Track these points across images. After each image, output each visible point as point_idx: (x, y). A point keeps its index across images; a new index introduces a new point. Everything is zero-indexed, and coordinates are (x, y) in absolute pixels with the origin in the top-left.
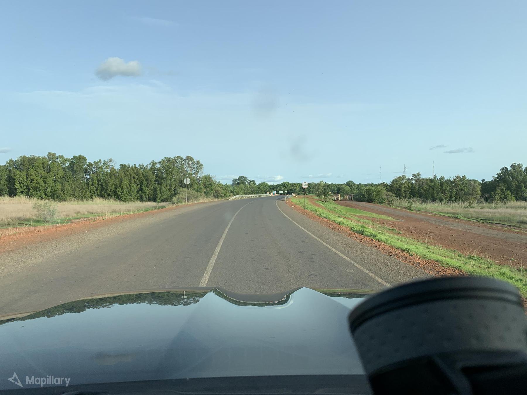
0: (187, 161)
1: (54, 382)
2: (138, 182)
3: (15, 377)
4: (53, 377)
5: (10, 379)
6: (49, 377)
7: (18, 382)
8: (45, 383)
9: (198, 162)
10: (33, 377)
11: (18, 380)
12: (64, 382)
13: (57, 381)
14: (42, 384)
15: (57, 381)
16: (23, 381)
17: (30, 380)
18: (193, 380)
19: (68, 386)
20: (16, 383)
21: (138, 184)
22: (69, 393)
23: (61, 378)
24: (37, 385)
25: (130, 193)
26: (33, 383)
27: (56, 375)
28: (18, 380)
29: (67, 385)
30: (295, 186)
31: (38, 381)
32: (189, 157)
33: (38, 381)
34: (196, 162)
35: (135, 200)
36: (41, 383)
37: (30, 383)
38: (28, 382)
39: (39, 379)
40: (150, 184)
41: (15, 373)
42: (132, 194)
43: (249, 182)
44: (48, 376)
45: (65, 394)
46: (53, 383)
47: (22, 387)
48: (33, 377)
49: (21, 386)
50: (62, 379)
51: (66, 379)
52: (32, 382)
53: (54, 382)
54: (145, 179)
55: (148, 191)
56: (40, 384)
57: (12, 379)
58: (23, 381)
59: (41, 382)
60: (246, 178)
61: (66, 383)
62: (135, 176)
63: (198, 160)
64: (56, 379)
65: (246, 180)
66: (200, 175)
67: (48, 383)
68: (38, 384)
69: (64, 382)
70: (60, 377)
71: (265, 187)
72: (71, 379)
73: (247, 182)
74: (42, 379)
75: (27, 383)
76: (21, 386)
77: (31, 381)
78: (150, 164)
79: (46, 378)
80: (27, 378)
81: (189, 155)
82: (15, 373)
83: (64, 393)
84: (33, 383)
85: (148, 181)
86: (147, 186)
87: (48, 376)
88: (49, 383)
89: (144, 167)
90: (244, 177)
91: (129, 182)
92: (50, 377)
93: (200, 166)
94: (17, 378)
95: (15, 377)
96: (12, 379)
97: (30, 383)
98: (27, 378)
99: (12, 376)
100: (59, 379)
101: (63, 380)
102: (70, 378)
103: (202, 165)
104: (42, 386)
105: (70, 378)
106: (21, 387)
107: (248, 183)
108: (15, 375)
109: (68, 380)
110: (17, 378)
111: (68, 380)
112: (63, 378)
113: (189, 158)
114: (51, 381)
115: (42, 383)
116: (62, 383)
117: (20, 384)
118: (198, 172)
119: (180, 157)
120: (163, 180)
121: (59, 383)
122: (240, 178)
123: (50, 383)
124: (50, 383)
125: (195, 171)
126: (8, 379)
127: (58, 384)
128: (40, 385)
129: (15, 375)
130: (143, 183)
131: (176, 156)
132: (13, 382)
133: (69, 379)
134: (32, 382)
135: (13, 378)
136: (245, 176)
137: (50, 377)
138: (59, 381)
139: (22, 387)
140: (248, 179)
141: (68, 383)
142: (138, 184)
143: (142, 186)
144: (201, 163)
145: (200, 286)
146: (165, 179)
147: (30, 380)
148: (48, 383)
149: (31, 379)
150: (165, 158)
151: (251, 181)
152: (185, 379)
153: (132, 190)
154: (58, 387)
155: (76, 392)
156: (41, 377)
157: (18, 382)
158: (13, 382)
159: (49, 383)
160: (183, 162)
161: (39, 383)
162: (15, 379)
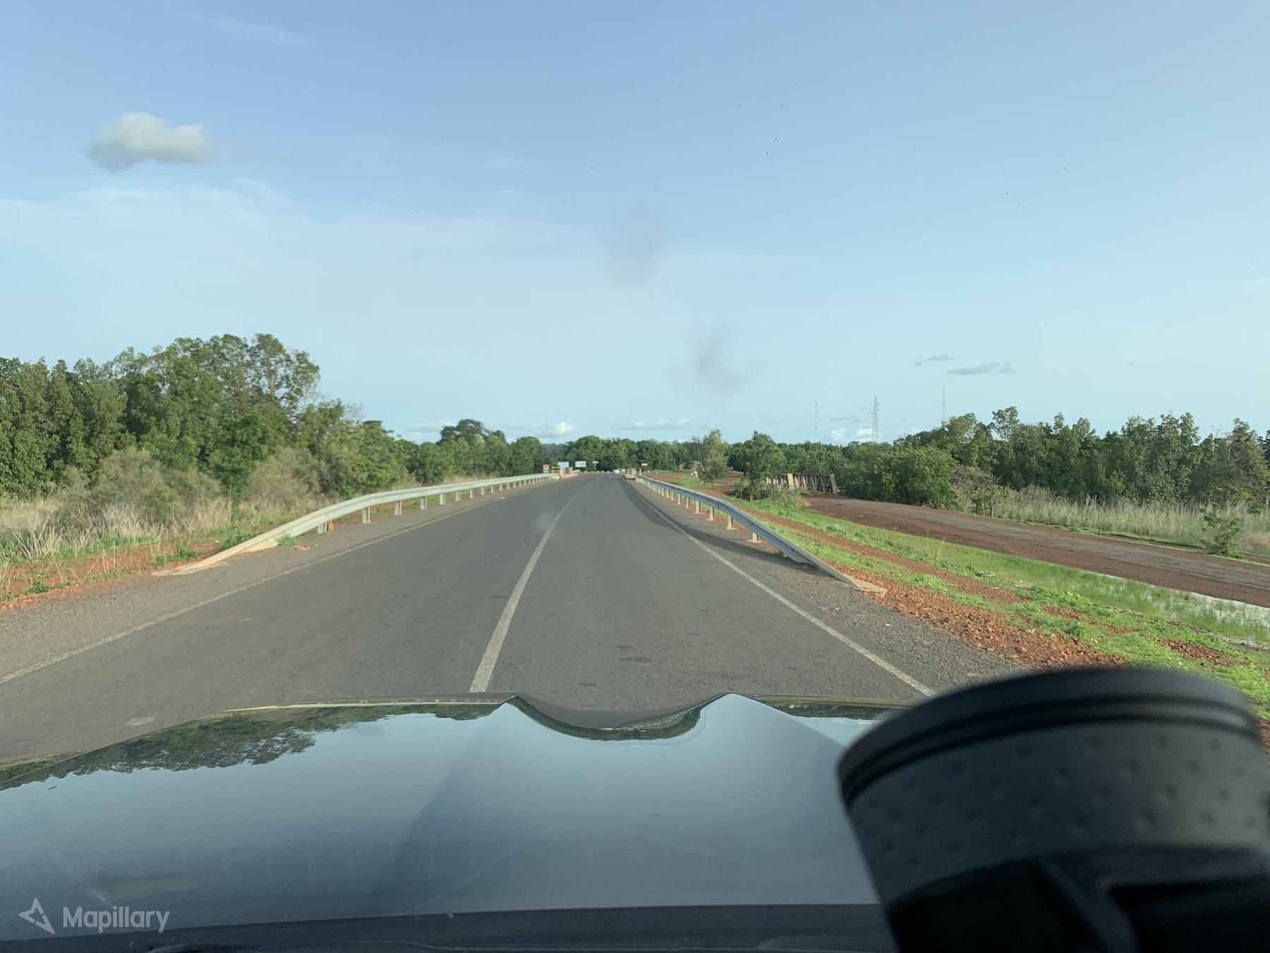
0: (262, 353)
1: (130, 922)
2: (51, 425)
3: (36, 910)
4: (127, 909)
5: (25, 915)
6: (118, 910)
7: (44, 923)
8: (107, 925)
9: (302, 357)
10: (80, 910)
11: (44, 917)
12: (154, 918)
13: (137, 919)
14: (101, 928)
15: (137, 919)
16: (56, 920)
18: (461, 916)
19: (165, 931)
20: (38, 924)
21: (51, 434)
22: (163, 949)
23: (148, 913)
24: (90, 928)
25: (11, 468)
26: (80, 925)
27: (135, 905)
28: (44, 917)
29: (161, 930)
30: (615, 446)
31: (90, 919)
32: (268, 336)
33: (90, 919)
34: (293, 358)
35: (34, 493)
36: (100, 926)
37: (73, 925)
39: (94, 914)
40: (100, 432)
41: (36, 900)
42: (22, 469)
43: (487, 434)
44: (115, 908)
45: (153, 951)
46: (127, 925)
47: (53, 932)
48: (80, 910)
50: (149, 914)
51: (159, 913)
52: (77, 920)
53: (130, 922)
54: (80, 414)
55: (90, 457)
57: (31, 916)
58: (56, 920)
59: (100, 922)
60: (478, 424)
61: (158, 925)
62: (40, 399)
63: (300, 352)
64: (135, 913)
65: (478, 431)
66: (302, 405)
68: (93, 927)
69: (154, 918)
70: (146, 908)
71: (532, 449)
72: (170, 914)
73: (483, 435)
74: (102, 914)
75: (65, 925)
77: (74, 919)
78: (118, 360)
79: (111, 911)
80: (66, 910)
81: (265, 333)
82: (36, 900)
83: (151, 948)
84: (80, 925)
85: (93, 421)
86: (88, 441)
87: (115, 908)
89: (97, 372)
90: (472, 422)
91: (9, 425)
92: (121, 908)
93: (306, 370)
94: (41, 911)
95: (36, 910)
96: (31, 916)
97: (73, 925)
98: (66, 910)
99: (29, 908)
100: (141, 914)
101: (152, 917)
102: (169, 912)
103: (315, 369)
104: (101, 931)
105: (169, 912)
106: (52, 934)
107: (486, 438)
108: (36, 904)
109: (163, 918)
110: (41, 911)
111: (163, 918)
112: (153, 913)
113: (268, 344)
114: (123, 919)
116: (148, 925)
117: (48, 927)
118: (299, 392)
119: (237, 339)
120: (153, 418)
121: (141, 925)
123: (121, 925)
124: (121, 925)
125: (287, 390)
126: (20, 915)
127: (140, 927)
128: (97, 928)
129: (36, 904)
130: (72, 429)
131: (221, 336)
132: (32, 920)
133: (167, 913)
134: (77, 920)
135: (32, 911)
138: (143, 920)
139: (53, 932)
141: (163, 923)
142: (51, 434)
143: (68, 439)
144: (310, 359)
145: (472, 690)
146: (161, 415)
147: (73, 917)
148: (115, 925)
150: (181, 341)
152: (445, 916)
153: (19, 454)
154: (137, 934)
155: (181, 946)
156: (99, 908)
157: (44, 923)
158: (32, 920)
160: (247, 358)
161: (94, 925)
162: (37, 916)
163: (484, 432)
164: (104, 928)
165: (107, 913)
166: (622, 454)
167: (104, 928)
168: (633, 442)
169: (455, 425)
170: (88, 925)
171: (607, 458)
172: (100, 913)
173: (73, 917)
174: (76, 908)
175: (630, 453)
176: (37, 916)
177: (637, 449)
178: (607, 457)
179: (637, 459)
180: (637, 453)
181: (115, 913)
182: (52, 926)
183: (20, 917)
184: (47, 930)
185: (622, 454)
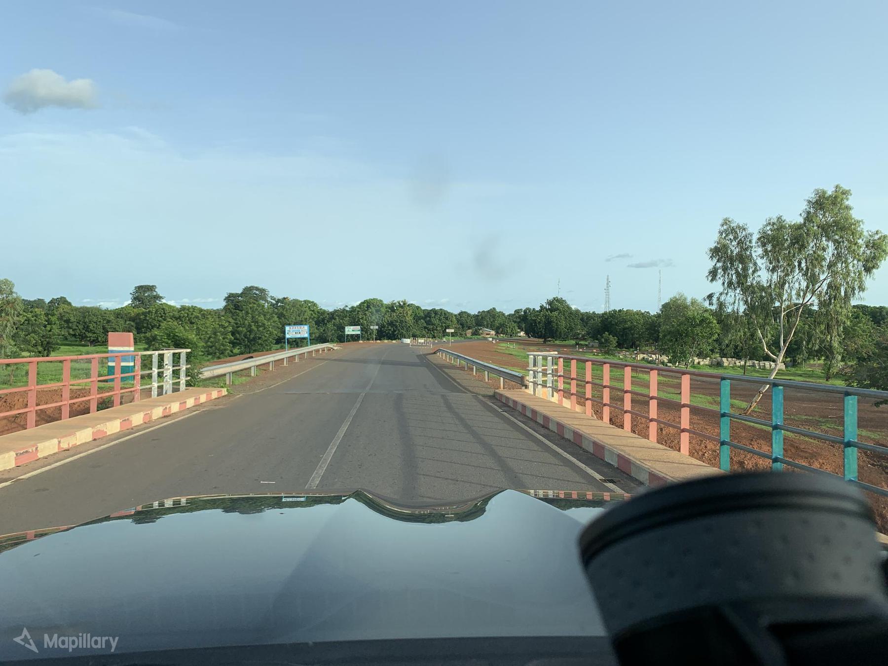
3: (25, 636)
5: (18, 640)
6: (82, 636)
7: (30, 645)
8: (75, 646)
10: (56, 636)
11: (31, 641)
16: (39, 644)
17: (51, 640)
20: (27, 646)
26: (56, 646)
28: (31, 641)
31: (63, 643)
33: (63, 643)
36: (70, 647)
37: (51, 647)
38: (48, 644)
39: (66, 639)
41: (25, 629)
43: (274, 302)
44: (80, 634)
48: (56, 636)
49: (36, 650)
56: (67, 647)
57: (21, 640)
58: (39, 644)
60: (263, 291)
67: (80, 646)
68: (65, 648)
74: (71, 639)
75: (46, 646)
76: (36, 650)
77: (52, 641)
79: (78, 637)
80: (46, 636)
82: (25, 629)
84: (56, 646)
88: (83, 647)
90: (257, 289)
94: (29, 637)
95: (25, 636)
96: (21, 640)
97: (51, 647)
98: (46, 636)
108: (25, 632)
110: (29, 637)
115: (71, 647)
117: (34, 648)
122: (248, 290)
126: (14, 639)
129: (25, 632)
135: (22, 637)
136: (261, 287)
137: (85, 635)
140: (271, 294)
147: (51, 641)
148: (80, 646)
149: (54, 637)
151: (279, 300)
157: (30, 645)
158: (23, 643)
159: (83, 647)
161: (66, 646)
162: (25, 640)
163: (269, 299)
164: (73, 648)
165: (75, 638)
166: (409, 319)
167: (73, 648)
168: (418, 308)
169: (240, 291)
170: (61, 646)
171: (391, 324)
172: (70, 638)
173: (51, 641)
174: (54, 634)
175: (417, 318)
176: (25, 640)
177: (422, 314)
178: (392, 322)
179: (425, 325)
180: (424, 318)
181: (80, 638)
182: (36, 646)
183: (15, 641)
184: (33, 650)
185: (409, 319)
